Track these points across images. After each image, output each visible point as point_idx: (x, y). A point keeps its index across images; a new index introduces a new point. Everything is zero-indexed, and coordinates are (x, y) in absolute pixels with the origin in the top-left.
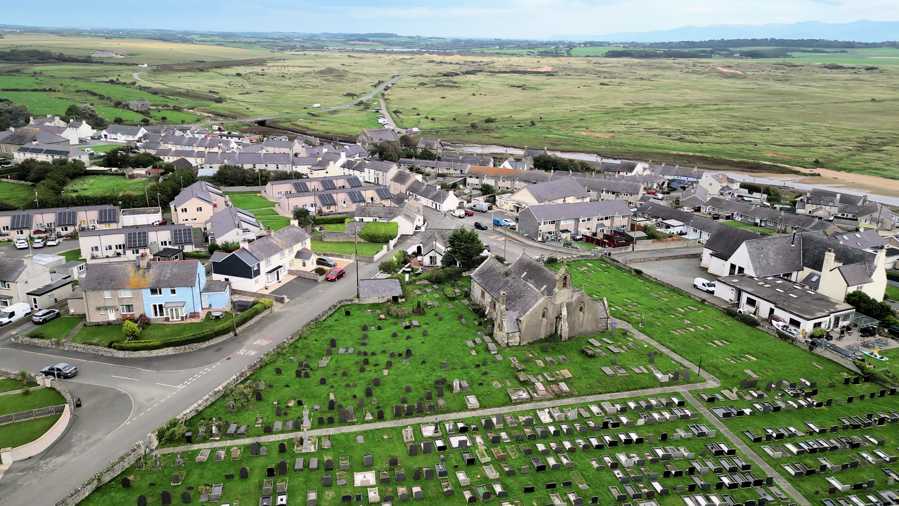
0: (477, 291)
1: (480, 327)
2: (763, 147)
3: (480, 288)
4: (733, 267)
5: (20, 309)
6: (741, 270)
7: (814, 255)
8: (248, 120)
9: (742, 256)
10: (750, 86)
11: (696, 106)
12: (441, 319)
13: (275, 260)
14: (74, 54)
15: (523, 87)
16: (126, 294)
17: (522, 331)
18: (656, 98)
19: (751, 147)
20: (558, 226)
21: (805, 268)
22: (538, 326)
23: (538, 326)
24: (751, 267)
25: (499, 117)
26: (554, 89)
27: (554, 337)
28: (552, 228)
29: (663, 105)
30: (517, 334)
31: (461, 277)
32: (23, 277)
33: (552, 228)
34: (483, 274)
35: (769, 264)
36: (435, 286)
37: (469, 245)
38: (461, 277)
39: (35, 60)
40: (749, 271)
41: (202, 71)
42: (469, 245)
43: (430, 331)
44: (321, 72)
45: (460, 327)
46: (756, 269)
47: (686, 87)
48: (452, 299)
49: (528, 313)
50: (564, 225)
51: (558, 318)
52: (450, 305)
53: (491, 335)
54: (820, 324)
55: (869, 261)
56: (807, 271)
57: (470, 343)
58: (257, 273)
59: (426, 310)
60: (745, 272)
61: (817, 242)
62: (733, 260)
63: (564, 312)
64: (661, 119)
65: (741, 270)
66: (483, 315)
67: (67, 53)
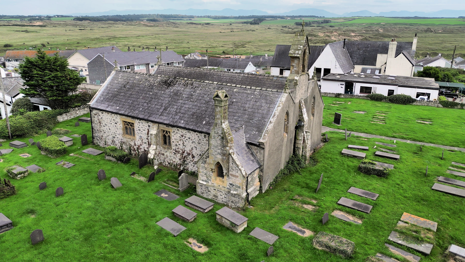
0: (110, 129)
1: (156, 184)
2: (193, 48)
3: (119, 119)
4: (318, 70)
6: (327, 71)
7: (360, 55)
9: (327, 59)
10: (163, 29)
11: (143, 36)
12: (59, 193)
15: (27, 31)
17: (265, 167)
18: (118, 34)
19: (188, 49)
21: (356, 66)
22: (279, 149)
24: (338, 66)
25: (14, 44)
26: (48, 32)
27: (295, 162)
29: (124, 36)
30: (256, 175)
31: (57, 123)
34: (114, 96)
36: (17, 142)
37: (59, 74)
38: (57, 123)
40: (336, 70)
42: (59, 74)
43: (46, 227)
45: (113, 197)
46: (342, 66)
47: (131, 30)
48: (62, 153)
49: (270, 127)
51: (299, 127)
52: (65, 162)
53: (191, 190)
55: (407, 48)
56: (358, 69)
57: (169, 225)
59: (15, 184)
60: (331, 72)
61: (359, 44)
62: (317, 64)
64: (129, 41)
65: (327, 71)
66: (144, 161)
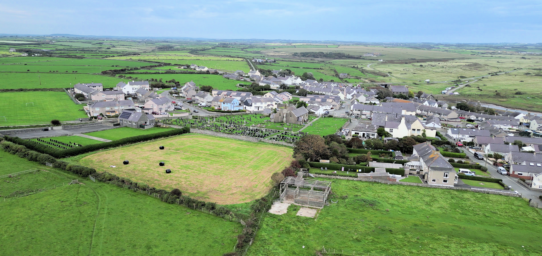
5: (203, 104)
8: (377, 84)
13: (258, 104)
14: (356, 55)
16: (219, 103)
20: (361, 112)
23: (278, 118)
28: (359, 113)
32: (206, 97)
33: (359, 113)
35: (380, 122)
39: (336, 57)
41: (406, 63)
44: (468, 65)
50: (364, 112)
54: (358, 133)
58: (251, 106)
63: (285, 115)
67: (351, 54)
